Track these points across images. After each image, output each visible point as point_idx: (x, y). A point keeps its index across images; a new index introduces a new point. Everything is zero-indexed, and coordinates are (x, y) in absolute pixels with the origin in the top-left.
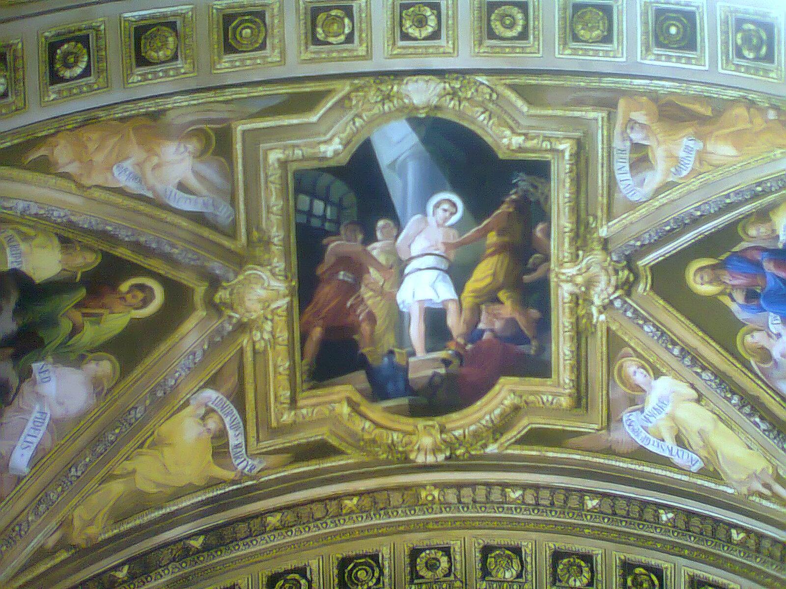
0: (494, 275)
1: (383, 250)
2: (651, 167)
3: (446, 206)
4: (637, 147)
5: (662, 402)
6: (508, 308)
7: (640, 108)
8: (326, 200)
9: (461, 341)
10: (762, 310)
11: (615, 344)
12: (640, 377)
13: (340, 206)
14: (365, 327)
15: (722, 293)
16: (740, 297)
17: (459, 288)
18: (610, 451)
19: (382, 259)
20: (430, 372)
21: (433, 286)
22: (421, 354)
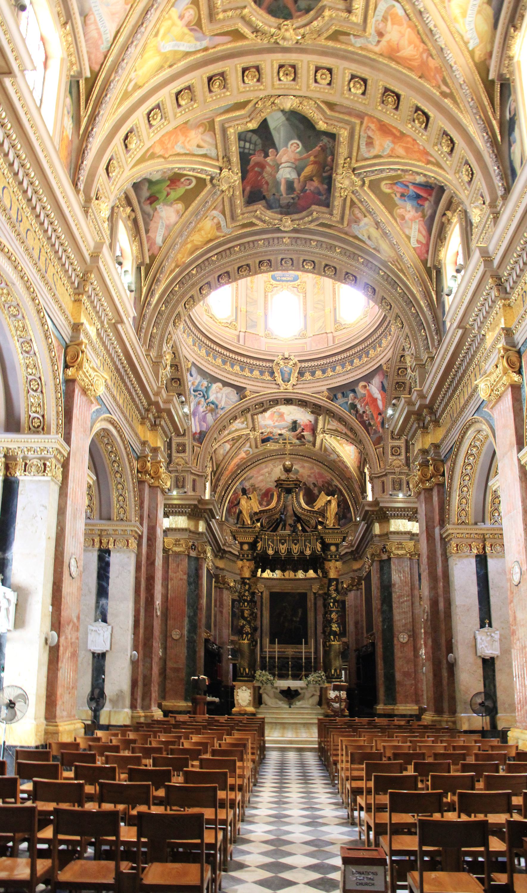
0: (312, 171)
1: (271, 160)
2: (374, 147)
3: (295, 145)
4: (369, 137)
5: (366, 224)
6: (316, 183)
7: (373, 123)
8: (250, 142)
9: (299, 192)
10: (405, 201)
11: (353, 203)
12: (359, 215)
13: (255, 144)
14: (265, 186)
15: (392, 193)
16: (398, 195)
17: (299, 175)
18: (346, 234)
19: (271, 163)
20: (287, 201)
21: (290, 173)
22: (284, 195)
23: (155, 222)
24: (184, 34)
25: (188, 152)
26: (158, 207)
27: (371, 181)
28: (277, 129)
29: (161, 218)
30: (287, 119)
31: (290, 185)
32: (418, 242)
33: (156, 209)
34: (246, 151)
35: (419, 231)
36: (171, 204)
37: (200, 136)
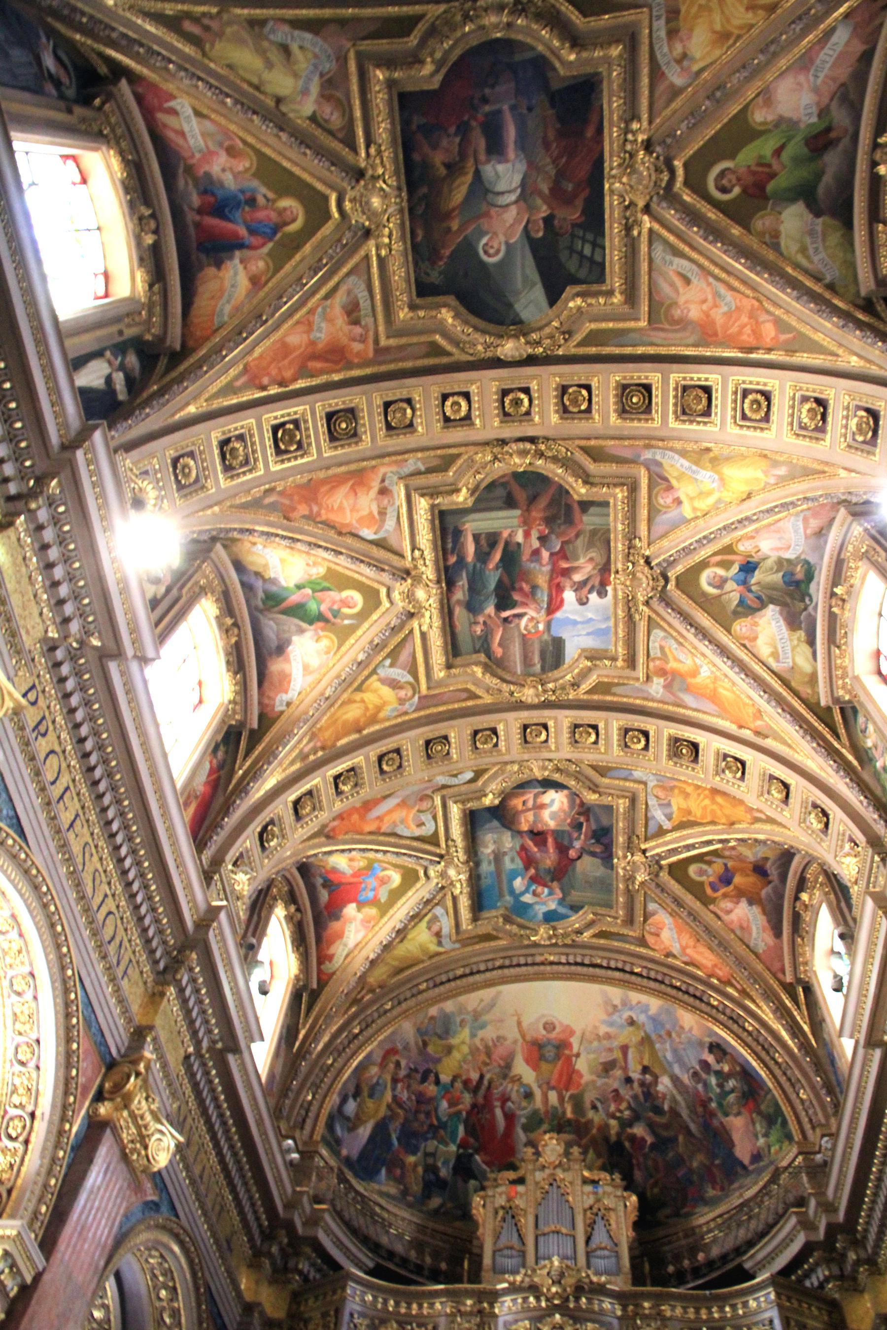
0: (450, 191)
1: (538, 209)
2: (343, 307)
3: (491, 251)
4: (356, 322)
6: (438, 159)
7: (358, 354)
8: (581, 254)
9: (474, 124)
10: (242, 191)
13: (572, 250)
14: (551, 135)
15: (274, 201)
16: (261, 201)
17: (478, 174)
19: (539, 201)
20: (498, 89)
21: (498, 176)
22: (506, 107)
23: (834, 79)
24: (678, 479)
25: (711, 280)
26: (814, 119)
27: (328, 216)
28: (528, 284)
29: (816, 90)
30: (510, 306)
31: (496, 149)
32: (174, 112)
33: (820, 116)
34: (590, 236)
35: (182, 134)
36: (780, 121)
37: (682, 300)
